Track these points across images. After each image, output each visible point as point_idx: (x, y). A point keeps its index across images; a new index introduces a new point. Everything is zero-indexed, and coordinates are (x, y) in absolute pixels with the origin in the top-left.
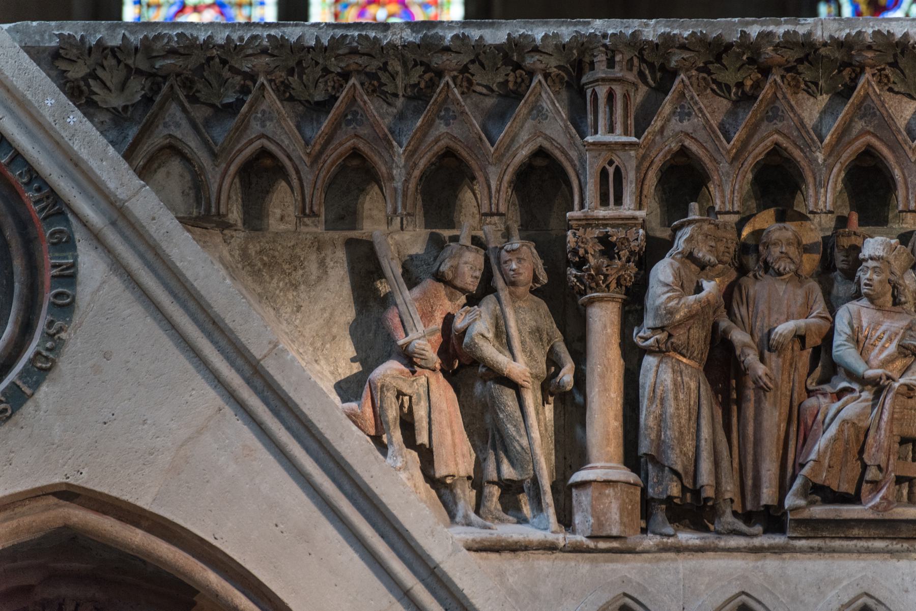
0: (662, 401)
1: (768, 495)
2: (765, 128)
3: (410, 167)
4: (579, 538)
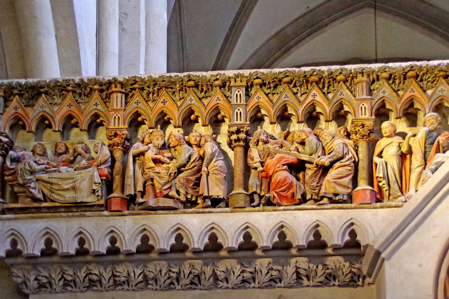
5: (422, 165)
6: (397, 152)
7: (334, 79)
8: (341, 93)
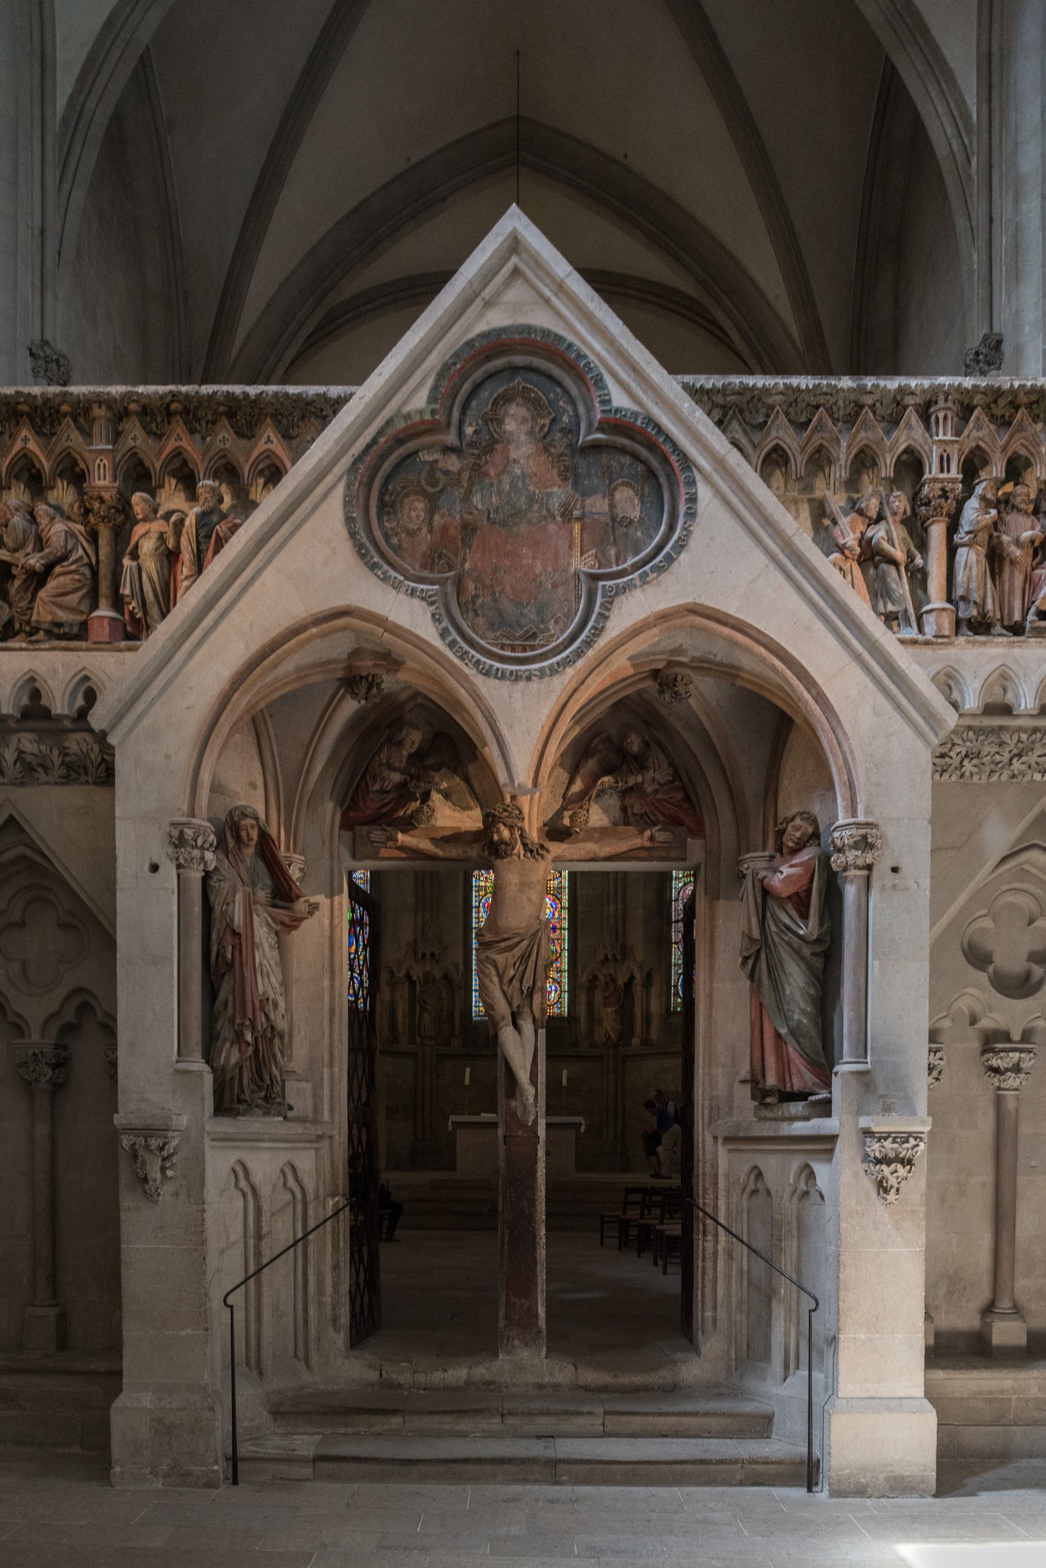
0: (971, 569)
1: (1017, 616)
2: (1017, 436)
3: (848, 454)
4: (929, 636)
5: (192, 576)
6: (156, 549)
7: (58, 411)
8: (68, 436)
